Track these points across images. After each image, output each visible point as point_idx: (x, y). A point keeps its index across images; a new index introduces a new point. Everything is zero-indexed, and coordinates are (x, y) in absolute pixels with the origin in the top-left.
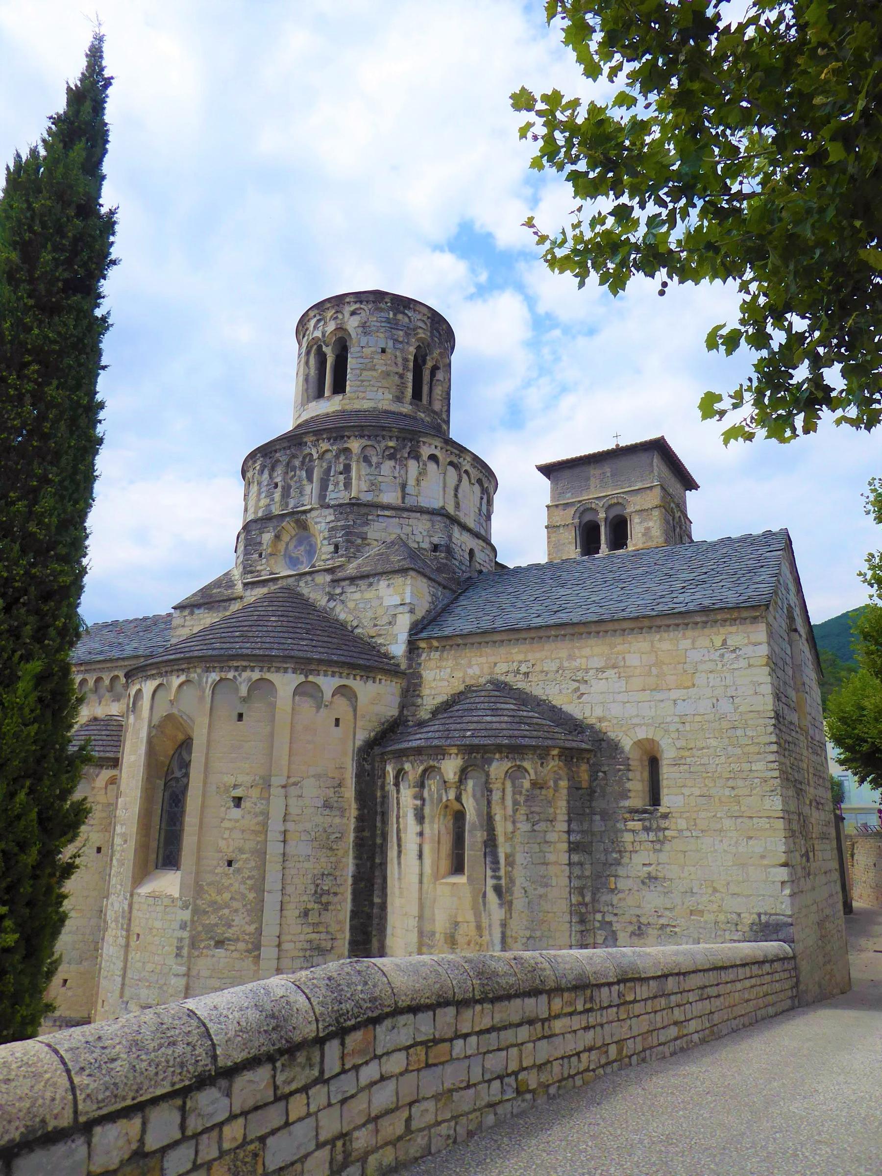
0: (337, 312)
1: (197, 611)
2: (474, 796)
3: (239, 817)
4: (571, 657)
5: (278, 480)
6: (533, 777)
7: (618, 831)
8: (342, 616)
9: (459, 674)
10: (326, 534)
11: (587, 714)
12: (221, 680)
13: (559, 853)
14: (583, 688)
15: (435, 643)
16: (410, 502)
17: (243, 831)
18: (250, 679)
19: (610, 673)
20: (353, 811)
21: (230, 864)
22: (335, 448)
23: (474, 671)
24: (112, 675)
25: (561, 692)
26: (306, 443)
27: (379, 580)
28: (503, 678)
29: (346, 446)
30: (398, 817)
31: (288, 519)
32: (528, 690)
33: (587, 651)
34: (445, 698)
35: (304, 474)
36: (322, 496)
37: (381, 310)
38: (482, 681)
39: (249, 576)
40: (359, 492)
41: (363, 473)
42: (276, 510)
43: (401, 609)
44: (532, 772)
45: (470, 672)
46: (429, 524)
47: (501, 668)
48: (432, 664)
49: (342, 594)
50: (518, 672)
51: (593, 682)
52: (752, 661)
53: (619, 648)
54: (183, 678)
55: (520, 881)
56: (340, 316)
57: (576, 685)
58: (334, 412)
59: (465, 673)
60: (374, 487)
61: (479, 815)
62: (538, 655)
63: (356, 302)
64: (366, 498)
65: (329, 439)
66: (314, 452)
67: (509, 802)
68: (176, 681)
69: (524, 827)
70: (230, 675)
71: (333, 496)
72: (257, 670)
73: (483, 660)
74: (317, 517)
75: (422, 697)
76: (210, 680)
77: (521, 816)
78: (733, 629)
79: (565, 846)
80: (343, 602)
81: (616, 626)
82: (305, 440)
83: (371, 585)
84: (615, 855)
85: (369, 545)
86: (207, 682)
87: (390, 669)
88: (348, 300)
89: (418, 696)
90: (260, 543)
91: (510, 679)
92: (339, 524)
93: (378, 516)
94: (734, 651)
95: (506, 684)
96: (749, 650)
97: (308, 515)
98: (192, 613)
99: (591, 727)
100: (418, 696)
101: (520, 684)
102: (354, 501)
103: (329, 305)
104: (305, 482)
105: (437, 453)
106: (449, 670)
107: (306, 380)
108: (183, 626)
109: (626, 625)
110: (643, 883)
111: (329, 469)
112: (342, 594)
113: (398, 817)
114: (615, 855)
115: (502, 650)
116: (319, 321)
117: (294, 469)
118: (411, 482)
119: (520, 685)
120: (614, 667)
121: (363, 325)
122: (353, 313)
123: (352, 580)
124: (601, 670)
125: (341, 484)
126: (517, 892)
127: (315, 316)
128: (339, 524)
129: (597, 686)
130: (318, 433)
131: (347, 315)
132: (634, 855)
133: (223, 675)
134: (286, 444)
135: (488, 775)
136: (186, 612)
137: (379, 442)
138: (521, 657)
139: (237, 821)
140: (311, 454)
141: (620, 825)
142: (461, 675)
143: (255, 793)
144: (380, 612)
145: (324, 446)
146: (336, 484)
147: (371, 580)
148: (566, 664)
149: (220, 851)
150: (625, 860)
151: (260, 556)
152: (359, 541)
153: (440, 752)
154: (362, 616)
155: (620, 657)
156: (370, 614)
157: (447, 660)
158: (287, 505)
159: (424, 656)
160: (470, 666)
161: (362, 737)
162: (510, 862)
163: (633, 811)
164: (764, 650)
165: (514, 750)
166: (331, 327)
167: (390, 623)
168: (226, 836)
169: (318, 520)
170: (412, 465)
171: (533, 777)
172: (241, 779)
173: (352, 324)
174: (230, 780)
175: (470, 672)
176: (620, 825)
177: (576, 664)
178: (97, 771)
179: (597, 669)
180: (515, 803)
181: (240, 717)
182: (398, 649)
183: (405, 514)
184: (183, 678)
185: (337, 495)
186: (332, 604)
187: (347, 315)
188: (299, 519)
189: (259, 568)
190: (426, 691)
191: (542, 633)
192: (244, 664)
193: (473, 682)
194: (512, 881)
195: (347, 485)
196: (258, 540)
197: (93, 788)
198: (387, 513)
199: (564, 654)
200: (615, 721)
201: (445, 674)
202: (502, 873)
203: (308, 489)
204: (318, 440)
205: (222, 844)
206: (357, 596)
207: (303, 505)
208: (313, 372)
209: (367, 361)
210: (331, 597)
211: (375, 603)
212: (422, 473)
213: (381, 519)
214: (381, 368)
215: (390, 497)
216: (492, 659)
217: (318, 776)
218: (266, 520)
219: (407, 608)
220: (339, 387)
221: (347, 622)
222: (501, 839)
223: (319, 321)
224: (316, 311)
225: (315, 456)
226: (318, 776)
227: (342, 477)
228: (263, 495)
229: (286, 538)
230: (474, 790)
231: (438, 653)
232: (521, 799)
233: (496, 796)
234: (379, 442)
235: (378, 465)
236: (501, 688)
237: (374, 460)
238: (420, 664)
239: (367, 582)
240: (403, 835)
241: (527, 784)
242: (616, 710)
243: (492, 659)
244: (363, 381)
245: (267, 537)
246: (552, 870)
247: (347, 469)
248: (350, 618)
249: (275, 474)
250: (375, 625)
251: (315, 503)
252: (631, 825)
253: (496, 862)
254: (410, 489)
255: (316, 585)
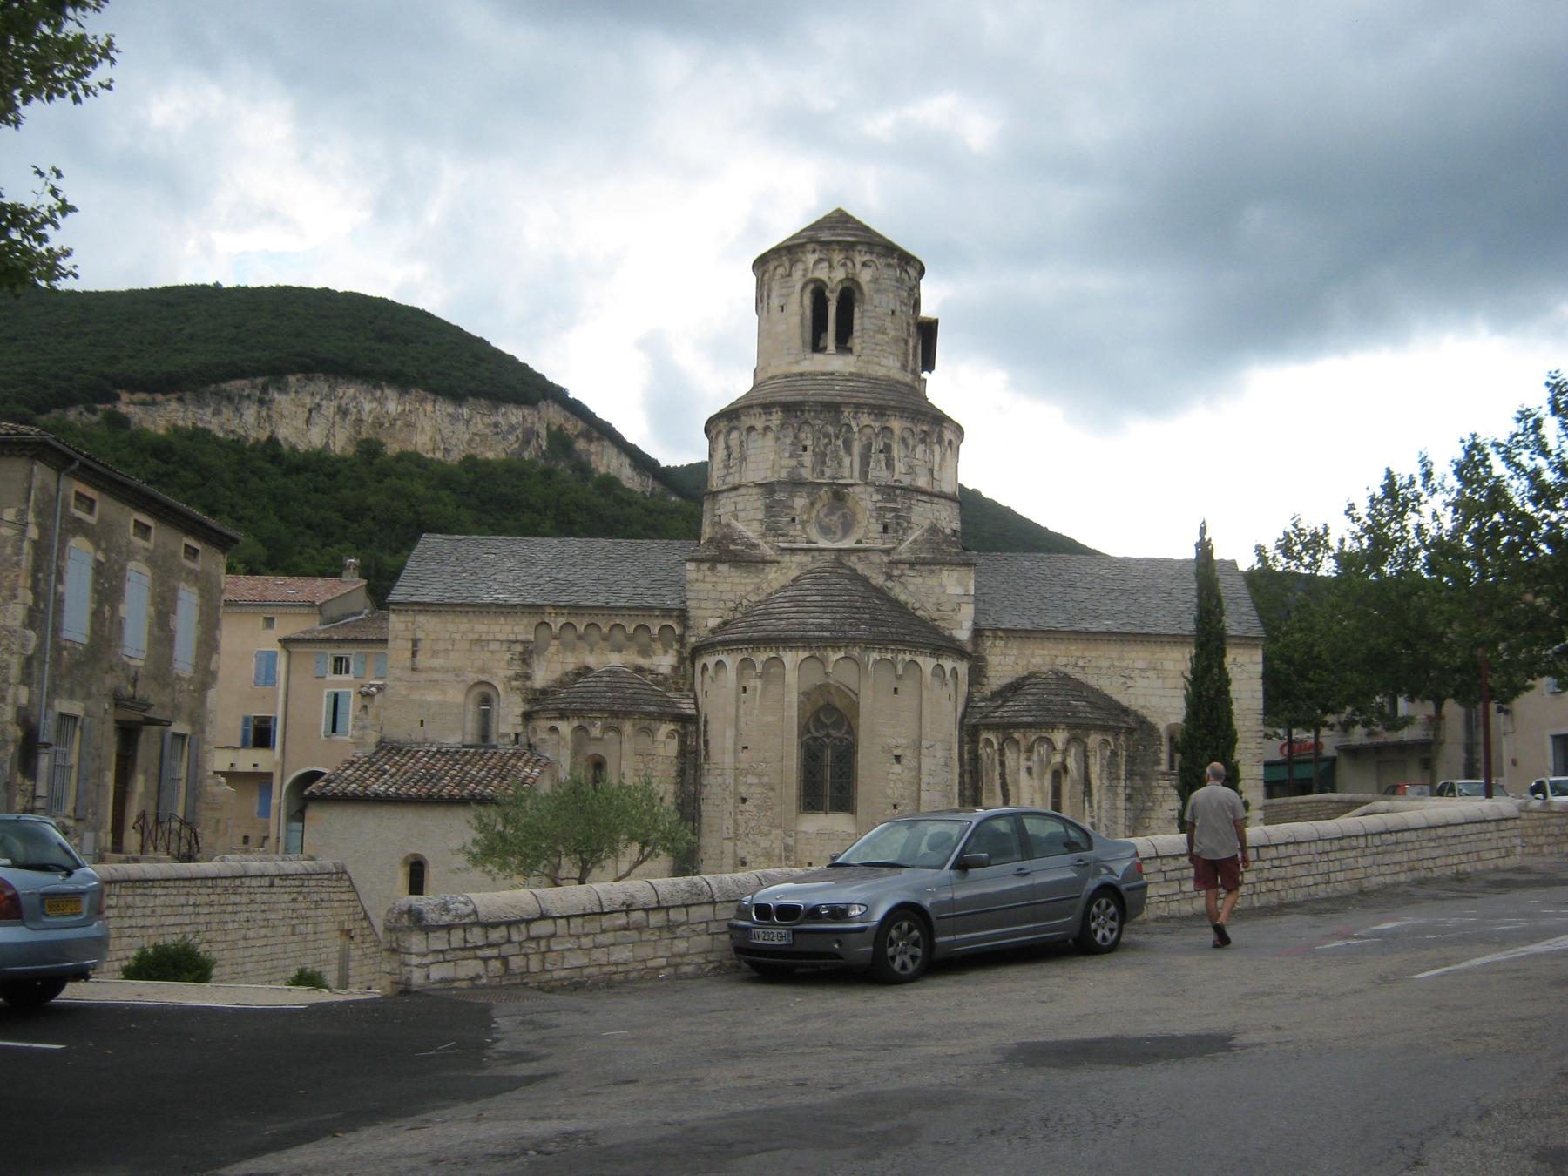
0: (847, 258)
1: (720, 567)
2: (1076, 761)
3: (900, 771)
4: (1121, 658)
5: (808, 443)
6: (1113, 747)
7: (1152, 788)
8: (902, 597)
9: (1022, 662)
10: (874, 514)
11: (1133, 702)
12: (881, 659)
13: (1121, 804)
14: (1130, 683)
15: (1000, 634)
16: (936, 490)
17: (903, 783)
18: (904, 659)
19: (1151, 674)
20: (957, 770)
21: (895, 807)
22: (877, 424)
23: (1037, 660)
24: (612, 623)
25: (1111, 684)
26: (842, 412)
27: (941, 570)
28: (1061, 669)
29: (887, 425)
30: (1003, 776)
31: (825, 488)
32: (1084, 680)
33: (1133, 655)
34: (1009, 680)
35: (840, 443)
36: (864, 473)
37: (888, 265)
38: (1045, 669)
39: (780, 539)
40: (900, 473)
41: (902, 454)
42: (806, 474)
43: (965, 599)
44: (1112, 744)
45: (1033, 661)
46: (950, 509)
47: (1062, 660)
48: (997, 651)
49: (900, 576)
50: (1076, 665)
51: (1139, 679)
52: (1252, 675)
53: (1158, 655)
54: (842, 654)
55: (1104, 820)
56: (849, 264)
57: (1124, 680)
58: (851, 374)
59: (1029, 662)
60: (911, 470)
61: (1079, 774)
62: (1094, 654)
63: (866, 252)
64: (906, 481)
65: (869, 414)
66: (853, 424)
67: (1098, 766)
68: (834, 657)
69: (1106, 783)
70: (889, 656)
71: (876, 474)
72: (908, 653)
73: (1045, 652)
74: (861, 493)
75: (987, 678)
76: (871, 660)
77: (1105, 776)
78: (1241, 651)
79: (1123, 797)
80: (903, 584)
81: (1159, 639)
82: (843, 409)
83: (933, 571)
84: (1150, 804)
85: (911, 528)
86: (869, 660)
87: (958, 651)
88: (859, 248)
89: (985, 677)
90: (791, 507)
91: (1069, 670)
92: (888, 505)
93: (918, 500)
94: (1240, 667)
95: (1066, 674)
96: (1250, 667)
97: (850, 489)
98: (713, 569)
99: (1135, 712)
100: (985, 677)
101: (1077, 675)
102: (897, 484)
103: (836, 247)
104: (842, 453)
105: (952, 438)
106: (1013, 658)
107: (802, 321)
108: (703, 581)
109: (1166, 639)
110: (1169, 822)
111: (868, 447)
112: (900, 576)
113: (1003, 776)
114: (1150, 804)
115: (1062, 647)
116: (820, 260)
117: (827, 435)
118: (936, 467)
119: (1078, 676)
120: (1155, 669)
121: (875, 280)
122: (864, 264)
123: (912, 565)
124: (1144, 670)
125: (883, 464)
126: (1102, 825)
127: (814, 251)
128: (888, 505)
129: (1140, 683)
130: (858, 407)
131: (858, 266)
132: (1164, 804)
133: (883, 655)
134: (819, 408)
135: (1086, 745)
136: (705, 566)
137: (916, 425)
138: (1078, 654)
139: (899, 774)
140: (849, 426)
141: (1154, 784)
142: (1025, 663)
143: (909, 753)
144: (943, 599)
145: (866, 419)
146: (879, 461)
147: (933, 567)
148: (1116, 663)
149: (888, 797)
150: (1157, 808)
151: (793, 520)
152: (905, 525)
153: (1053, 727)
154: (924, 599)
155: (1159, 663)
156: (933, 599)
157: (1012, 648)
158: (822, 473)
159: (989, 643)
160: (1033, 655)
161: (960, 709)
162: (1099, 808)
163: (1163, 774)
164: (1260, 668)
165: (1104, 729)
166: (840, 274)
167: (954, 610)
168: (892, 785)
169: (863, 496)
170: (937, 448)
171: (1113, 747)
172: (903, 741)
173: (865, 276)
174: (892, 742)
175: (1033, 661)
176: (1154, 784)
177: (1125, 663)
178: (658, 724)
179: (1142, 670)
180: (1102, 766)
181: (896, 690)
182: (963, 634)
183: (936, 500)
184: (842, 654)
185: (878, 473)
186: (889, 584)
187: (858, 266)
188: (839, 494)
189: (791, 533)
190: (991, 673)
191: (1098, 637)
192: (900, 647)
193: (1035, 669)
194: (1099, 819)
195: (890, 464)
196: (790, 503)
197: (654, 741)
198: (924, 498)
199: (1114, 655)
200: (1153, 709)
201: (1010, 660)
202: (1095, 814)
203: (847, 461)
204: (856, 413)
205: (889, 792)
206: (918, 580)
207: (843, 478)
208: (808, 313)
209: (880, 323)
210: (889, 577)
211: (938, 590)
212: (943, 459)
213: (920, 504)
214: (892, 333)
215: (922, 482)
216: (1053, 652)
217: (942, 741)
218: (795, 484)
219: (971, 599)
220: (844, 341)
221: (907, 603)
222: (1095, 791)
223: (820, 260)
224: (818, 248)
225: (856, 429)
226: (942, 741)
227: (882, 455)
228: (787, 454)
229: (818, 506)
230: (1075, 755)
231: (1002, 642)
232: (1105, 763)
233: (1091, 761)
234: (916, 425)
235: (914, 448)
236: (1064, 680)
237: (911, 442)
238: (985, 650)
239: (927, 567)
240: (1012, 789)
241: (1108, 753)
242: (1154, 701)
243: (1053, 652)
244: (876, 344)
245: (800, 502)
246: (1119, 811)
247: (887, 449)
248: (911, 600)
249: (802, 436)
250: (939, 610)
251: (856, 478)
252: (1162, 783)
253: (1091, 806)
254: (936, 475)
255: (872, 563)
